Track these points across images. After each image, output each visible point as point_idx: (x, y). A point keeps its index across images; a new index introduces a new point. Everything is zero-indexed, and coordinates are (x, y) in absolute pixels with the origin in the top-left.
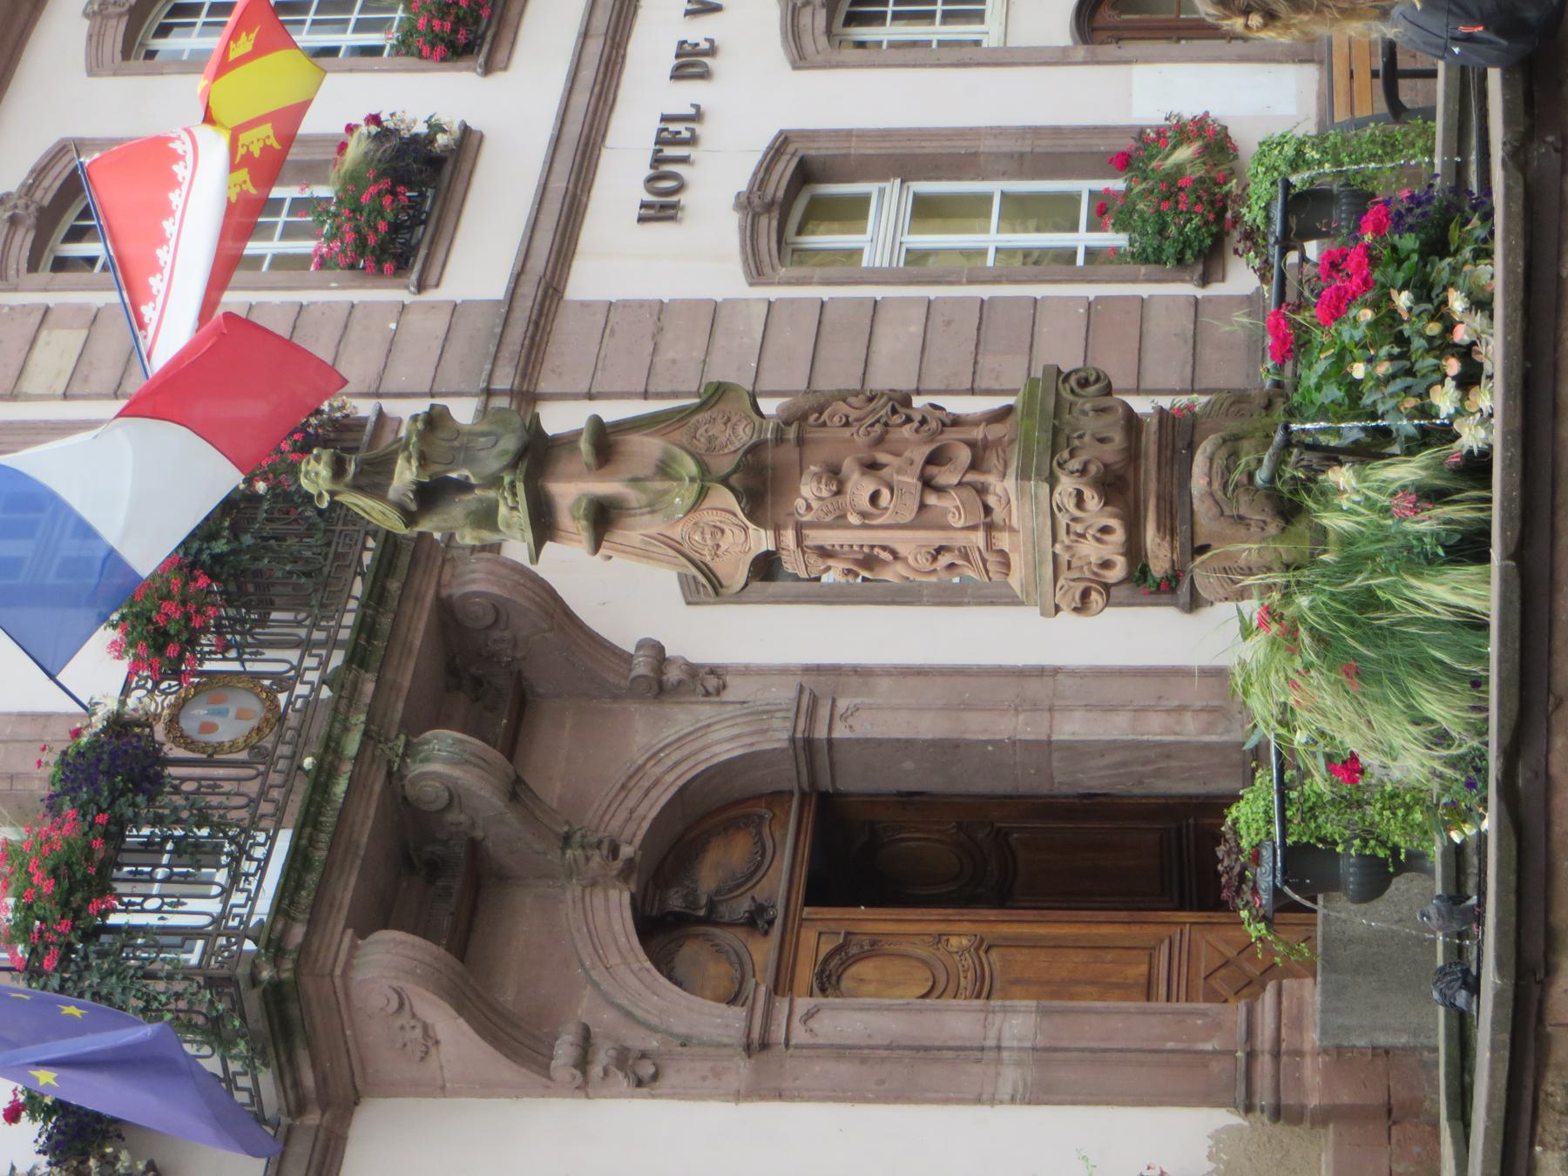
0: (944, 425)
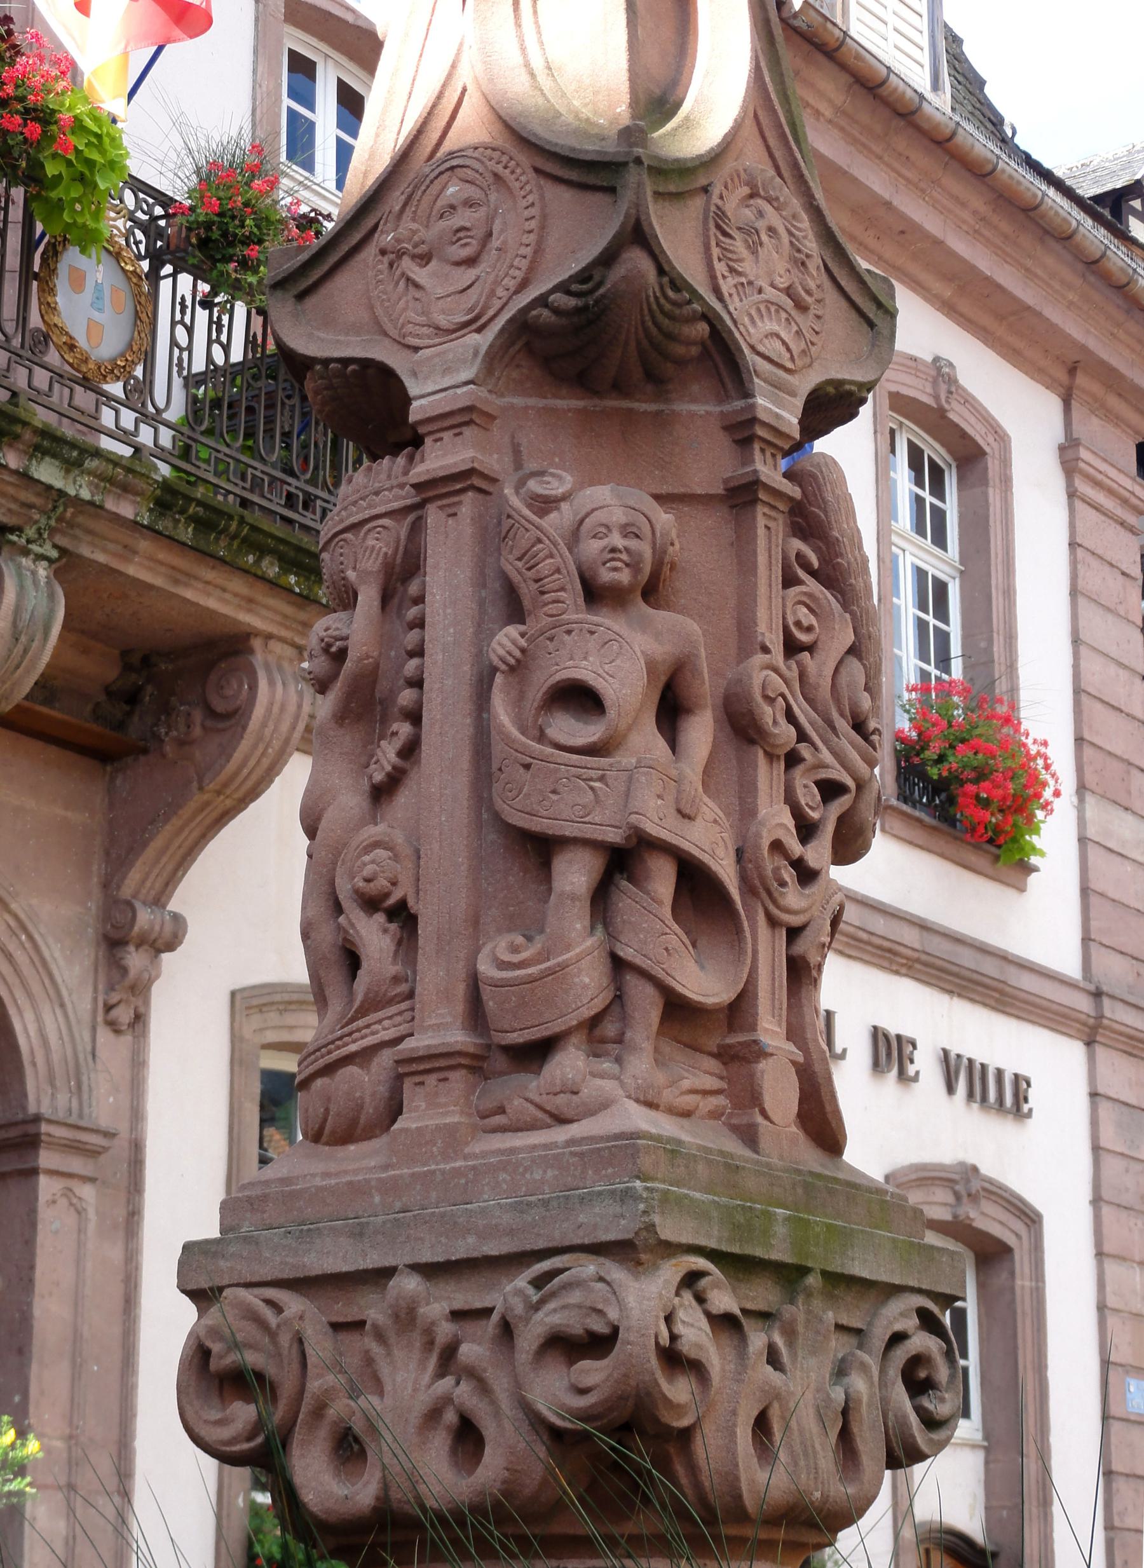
0: (794, 933)
